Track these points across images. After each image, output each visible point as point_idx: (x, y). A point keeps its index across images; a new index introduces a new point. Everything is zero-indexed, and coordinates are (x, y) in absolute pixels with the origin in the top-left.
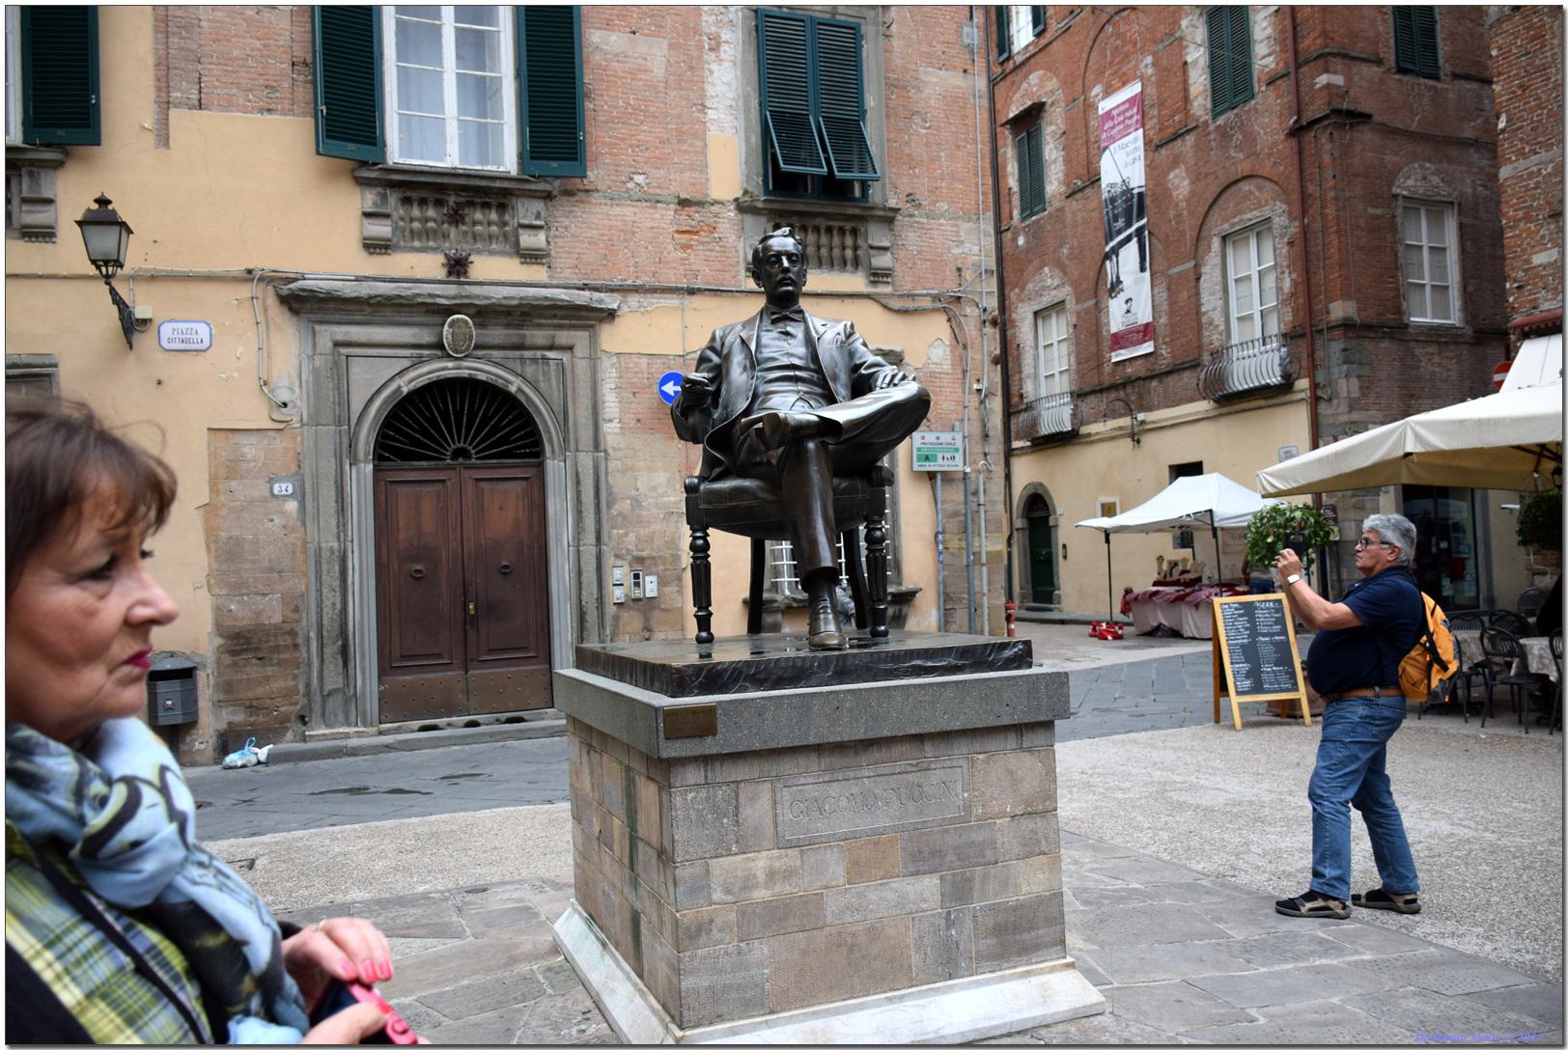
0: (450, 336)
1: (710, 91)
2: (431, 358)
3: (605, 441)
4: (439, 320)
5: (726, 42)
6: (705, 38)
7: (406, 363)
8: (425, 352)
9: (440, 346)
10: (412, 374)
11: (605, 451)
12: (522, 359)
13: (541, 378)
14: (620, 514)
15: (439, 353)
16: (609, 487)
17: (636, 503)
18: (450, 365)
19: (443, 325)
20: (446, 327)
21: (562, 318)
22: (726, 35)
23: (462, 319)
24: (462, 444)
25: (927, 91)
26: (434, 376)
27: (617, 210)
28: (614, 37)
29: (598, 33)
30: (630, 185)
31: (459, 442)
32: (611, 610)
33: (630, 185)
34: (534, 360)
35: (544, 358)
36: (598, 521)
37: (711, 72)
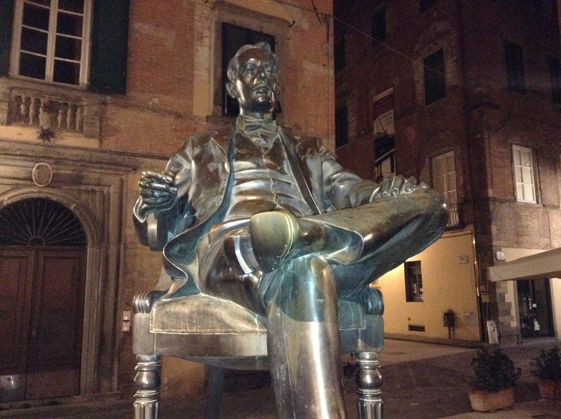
0: (36, 174)
1: (196, 60)
2: (25, 186)
3: (125, 238)
4: (31, 164)
5: (206, 37)
6: (196, 34)
7: (9, 188)
8: (21, 182)
9: (30, 179)
10: (11, 194)
11: (125, 244)
12: (79, 191)
13: (90, 201)
14: (131, 280)
15: (29, 183)
16: (125, 264)
17: (141, 274)
18: (35, 190)
19: (33, 167)
20: (34, 169)
21: (107, 169)
22: (206, 33)
23: (47, 166)
24: (35, 236)
25: (306, 73)
26: (24, 197)
27: (142, 115)
28: (147, 27)
29: (140, 24)
30: (151, 103)
31: (37, 235)
32: (119, 337)
33: (151, 103)
34: (88, 192)
35: (93, 190)
36: (117, 285)
37: (198, 51)
